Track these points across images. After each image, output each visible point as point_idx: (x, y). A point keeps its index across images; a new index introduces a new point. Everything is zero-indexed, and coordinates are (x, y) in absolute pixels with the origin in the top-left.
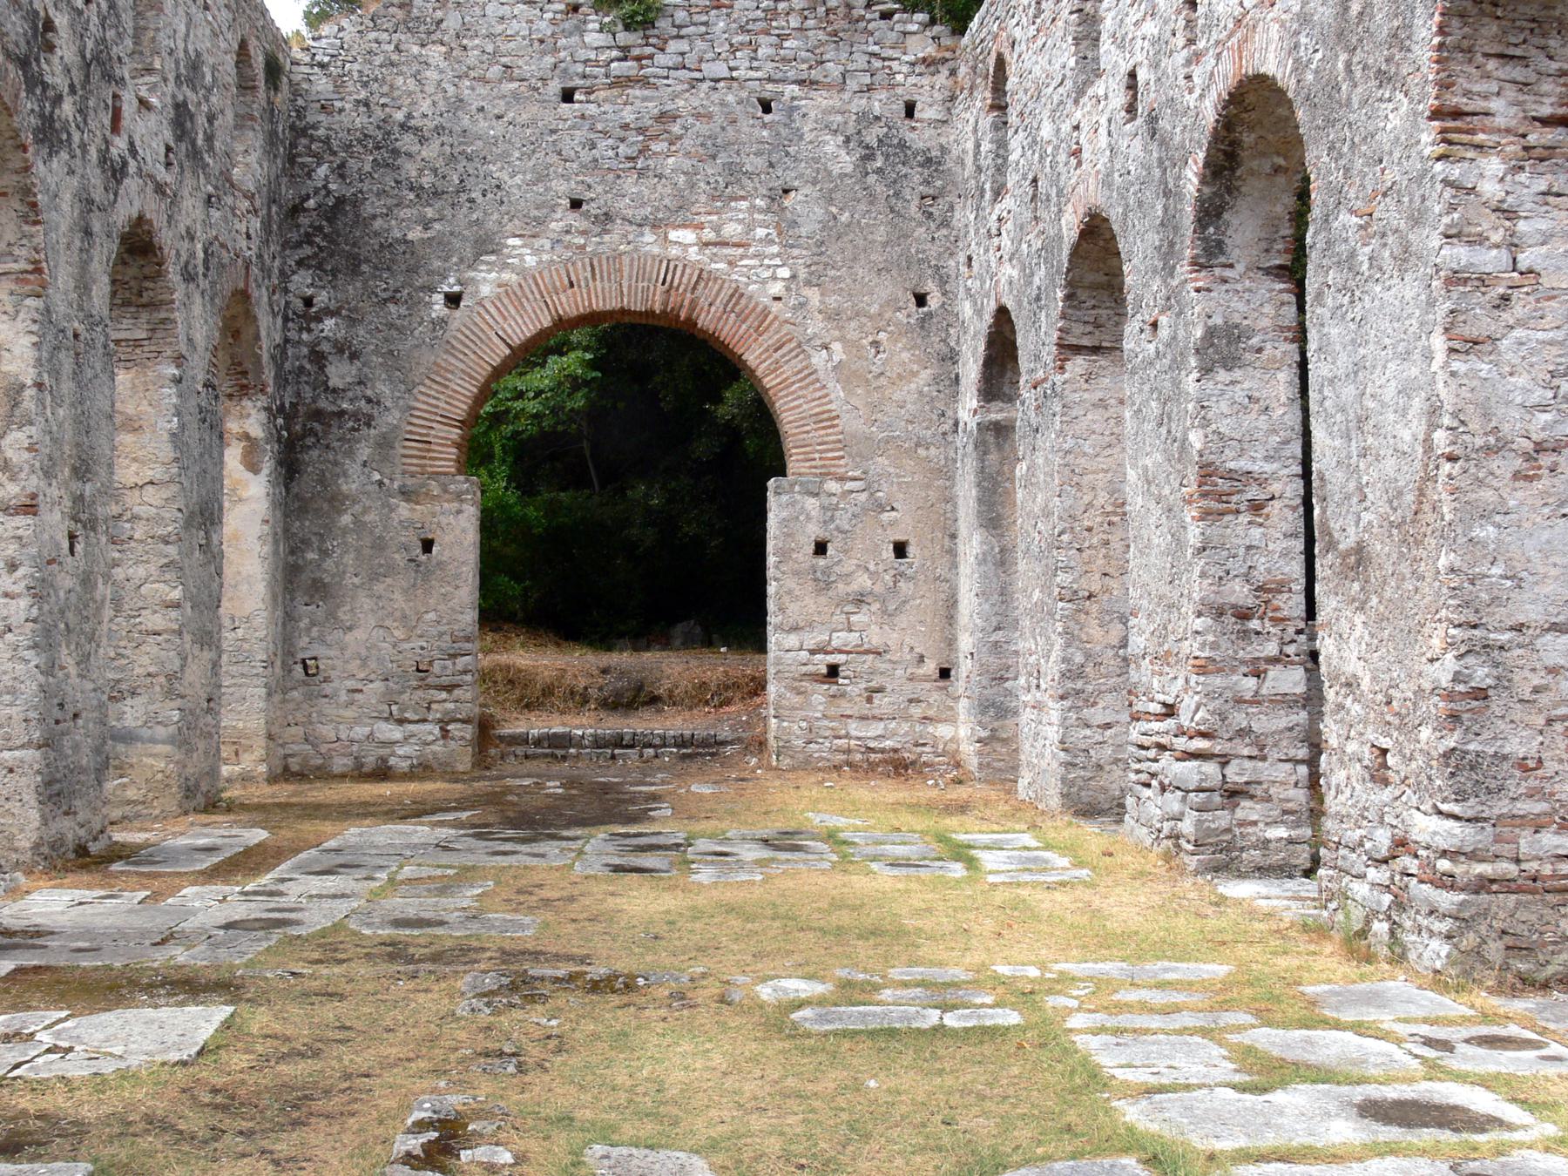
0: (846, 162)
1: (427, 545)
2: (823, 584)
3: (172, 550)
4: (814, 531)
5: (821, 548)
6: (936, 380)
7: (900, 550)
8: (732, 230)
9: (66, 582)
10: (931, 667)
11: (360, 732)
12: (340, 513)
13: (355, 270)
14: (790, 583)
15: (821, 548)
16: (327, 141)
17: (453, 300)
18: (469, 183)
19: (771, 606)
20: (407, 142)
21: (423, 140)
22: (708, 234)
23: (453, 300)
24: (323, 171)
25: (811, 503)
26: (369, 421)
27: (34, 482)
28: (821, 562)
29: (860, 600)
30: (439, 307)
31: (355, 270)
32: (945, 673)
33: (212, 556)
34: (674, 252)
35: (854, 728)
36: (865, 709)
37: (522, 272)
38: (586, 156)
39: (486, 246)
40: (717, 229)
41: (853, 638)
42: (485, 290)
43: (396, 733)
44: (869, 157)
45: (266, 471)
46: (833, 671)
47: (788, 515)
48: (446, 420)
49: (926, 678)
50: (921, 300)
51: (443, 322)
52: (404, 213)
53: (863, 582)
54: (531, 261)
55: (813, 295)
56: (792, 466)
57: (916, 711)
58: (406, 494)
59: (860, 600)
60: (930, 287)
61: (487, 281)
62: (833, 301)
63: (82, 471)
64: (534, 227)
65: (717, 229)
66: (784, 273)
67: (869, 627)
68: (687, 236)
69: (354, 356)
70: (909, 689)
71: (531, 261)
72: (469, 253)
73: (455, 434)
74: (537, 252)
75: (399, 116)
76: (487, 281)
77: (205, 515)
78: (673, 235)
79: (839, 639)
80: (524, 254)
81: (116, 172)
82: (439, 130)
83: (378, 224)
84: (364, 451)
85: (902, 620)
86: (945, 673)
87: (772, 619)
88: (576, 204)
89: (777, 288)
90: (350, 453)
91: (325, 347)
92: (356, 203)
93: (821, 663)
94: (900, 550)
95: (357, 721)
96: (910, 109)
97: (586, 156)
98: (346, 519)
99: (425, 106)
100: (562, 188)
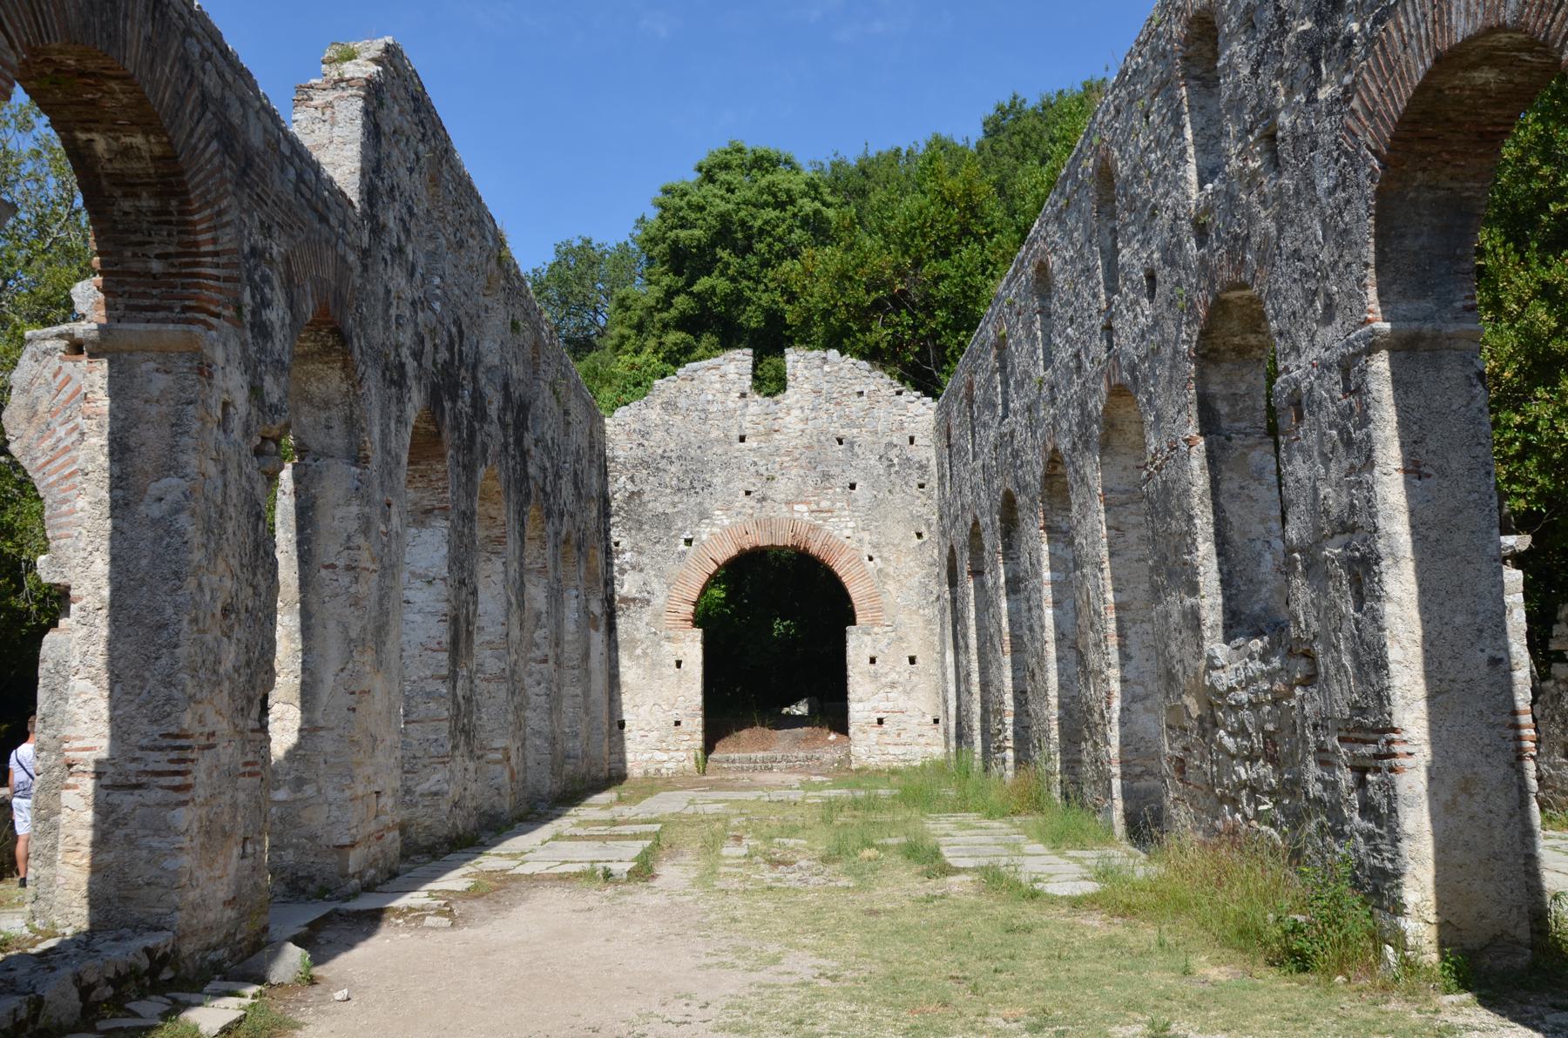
0: (881, 468)
1: (679, 664)
2: (875, 677)
3: (576, 672)
4: (869, 652)
5: (873, 661)
6: (928, 575)
7: (912, 660)
8: (825, 504)
9: (555, 689)
10: (930, 719)
11: (646, 756)
12: (635, 648)
13: (640, 529)
14: (858, 678)
15: (873, 661)
16: (624, 465)
17: (689, 542)
18: (696, 484)
19: (850, 689)
20: (663, 464)
21: (672, 463)
22: (814, 507)
23: (689, 542)
24: (623, 479)
25: (867, 638)
26: (648, 602)
27: (547, 651)
28: (872, 667)
29: (893, 685)
30: (682, 547)
31: (640, 529)
32: (936, 721)
33: (588, 672)
34: (797, 515)
35: (891, 749)
36: (898, 740)
37: (722, 528)
38: (753, 469)
39: (704, 515)
40: (818, 504)
41: (890, 705)
42: (704, 537)
43: (665, 757)
44: (892, 465)
45: (602, 629)
46: (880, 721)
47: (858, 646)
48: (686, 601)
49: (927, 724)
50: (919, 535)
51: (684, 553)
52: (663, 499)
53: (893, 676)
54: (726, 522)
55: (866, 536)
56: (858, 620)
57: (922, 740)
58: (668, 638)
59: (893, 685)
60: (923, 529)
61: (705, 533)
62: (875, 539)
63: (557, 645)
64: (727, 508)
65: (818, 504)
66: (851, 524)
67: (898, 699)
68: (803, 508)
69: (641, 570)
70: (918, 730)
71: (726, 522)
72: (696, 519)
73: (692, 609)
74: (729, 517)
75: (660, 451)
76: (705, 533)
77: (586, 656)
78: (796, 507)
79: (882, 706)
80: (722, 519)
81: (562, 515)
82: (679, 458)
83: (650, 506)
84: (646, 618)
85: (913, 695)
86: (936, 721)
87: (851, 696)
88: (748, 493)
89: (847, 532)
90: (640, 619)
91: (627, 567)
92: (640, 493)
93: (874, 718)
94: (912, 660)
95: (645, 751)
96: (912, 440)
97: (753, 469)
98: (639, 651)
99: (672, 446)
100: (739, 486)
